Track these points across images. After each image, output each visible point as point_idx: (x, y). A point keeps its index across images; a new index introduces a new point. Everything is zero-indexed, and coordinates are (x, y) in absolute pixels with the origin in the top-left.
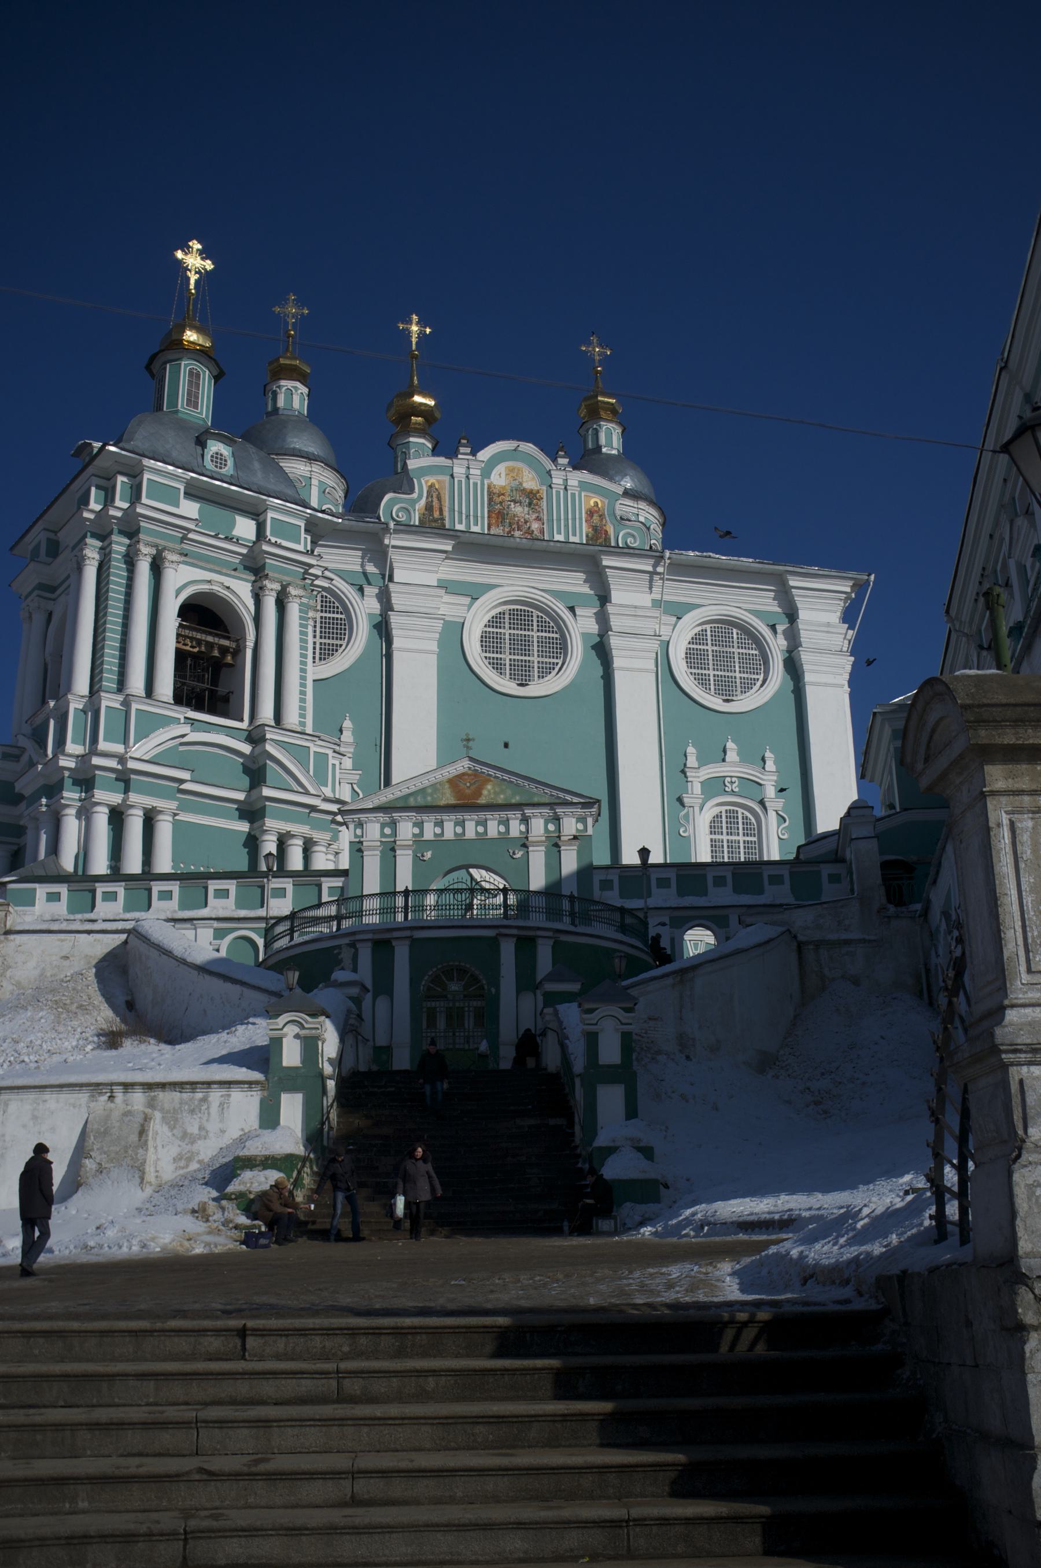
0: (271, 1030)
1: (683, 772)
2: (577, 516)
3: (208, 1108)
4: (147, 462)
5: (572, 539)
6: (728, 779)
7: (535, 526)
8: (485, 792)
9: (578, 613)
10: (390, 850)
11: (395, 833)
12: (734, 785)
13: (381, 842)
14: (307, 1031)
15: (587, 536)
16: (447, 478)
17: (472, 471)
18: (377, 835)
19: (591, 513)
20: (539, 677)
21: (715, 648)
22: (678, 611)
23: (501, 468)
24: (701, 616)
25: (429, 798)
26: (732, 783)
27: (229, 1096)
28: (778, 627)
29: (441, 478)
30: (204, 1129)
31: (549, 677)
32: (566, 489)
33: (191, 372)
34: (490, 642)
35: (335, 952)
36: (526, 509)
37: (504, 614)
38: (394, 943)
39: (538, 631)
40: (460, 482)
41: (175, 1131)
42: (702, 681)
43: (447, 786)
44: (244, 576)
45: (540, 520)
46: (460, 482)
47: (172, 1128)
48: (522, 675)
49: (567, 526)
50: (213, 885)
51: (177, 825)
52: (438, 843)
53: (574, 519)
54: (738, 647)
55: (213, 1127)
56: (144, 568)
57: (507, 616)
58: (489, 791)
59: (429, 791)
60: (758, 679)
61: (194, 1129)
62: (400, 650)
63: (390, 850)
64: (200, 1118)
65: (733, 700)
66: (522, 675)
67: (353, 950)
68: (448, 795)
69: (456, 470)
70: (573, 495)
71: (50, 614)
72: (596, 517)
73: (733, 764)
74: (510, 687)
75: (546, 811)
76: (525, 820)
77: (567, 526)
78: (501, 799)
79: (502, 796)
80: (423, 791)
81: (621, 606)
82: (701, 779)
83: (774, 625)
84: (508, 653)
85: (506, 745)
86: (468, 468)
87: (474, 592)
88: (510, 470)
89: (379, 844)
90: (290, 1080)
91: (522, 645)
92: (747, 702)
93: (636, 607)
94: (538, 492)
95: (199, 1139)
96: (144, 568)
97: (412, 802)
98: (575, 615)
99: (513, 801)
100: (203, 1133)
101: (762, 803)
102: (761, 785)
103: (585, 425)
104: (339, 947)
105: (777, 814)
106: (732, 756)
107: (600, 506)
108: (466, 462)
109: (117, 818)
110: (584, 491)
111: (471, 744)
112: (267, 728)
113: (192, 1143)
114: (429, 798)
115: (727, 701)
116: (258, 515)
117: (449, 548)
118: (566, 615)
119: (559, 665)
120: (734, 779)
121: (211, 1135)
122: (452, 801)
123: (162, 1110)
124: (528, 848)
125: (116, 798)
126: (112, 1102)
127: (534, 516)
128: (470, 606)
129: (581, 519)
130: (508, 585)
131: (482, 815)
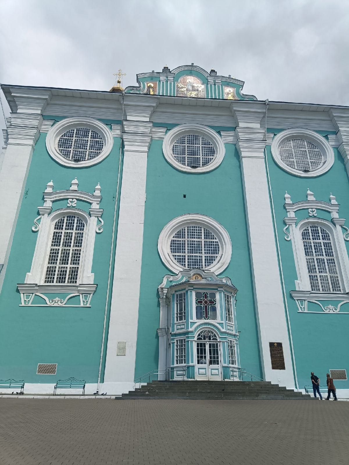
1: (285, 208)
6: (311, 210)
12: (314, 213)
22: (275, 131)
26: (313, 211)
32: (215, 85)
42: (291, 165)
48: (194, 164)
62: (127, 151)
66: (194, 164)
73: (312, 201)
82: (295, 210)
85: (185, 196)
87: (168, 127)
98: (221, 135)
101: (333, 222)
102: (329, 212)
105: (342, 227)
106: (310, 198)
117: (154, 105)
120: (313, 210)
128: (166, 132)
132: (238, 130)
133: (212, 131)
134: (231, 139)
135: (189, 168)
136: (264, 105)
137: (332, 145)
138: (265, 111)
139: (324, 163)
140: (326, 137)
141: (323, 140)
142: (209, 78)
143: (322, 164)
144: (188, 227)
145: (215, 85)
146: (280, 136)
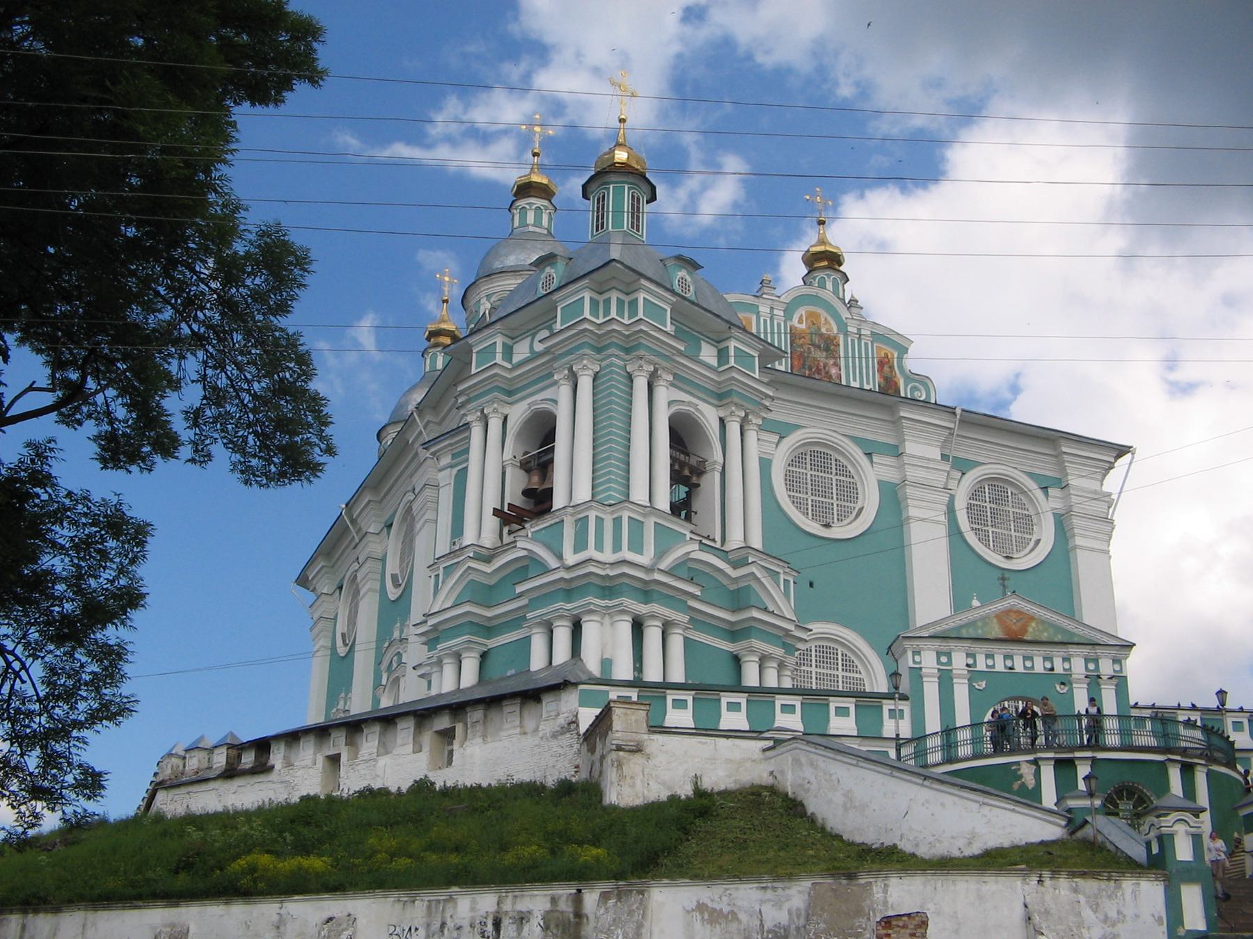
0: (1200, 827)
2: (871, 366)
3: (1123, 894)
4: (643, 282)
5: (853, 384)
7: (833, 371)
8: (1030, 629)
9: (874, 460)
10: (946, 680)
11: (950, 662)
13: (939, 670)
14: (1192, 829)
15: (879, 386)
16: (754, 318)
17: (776, 312)
18: (933, 662)
19: (881, 364)
20: (838, 519)
21: (992, 506)
22: (962, 466)
23: (802, 311)
24: (978, 475)
25: (980, 631)
27: (1139, 884)
28: (1049, 490)
29: (747, 315)
30: (1122, 913)
31: (848, 520)
32: (859, 339)
33: (633, 196)
34: (792, 482)
35: (1013, 768)
36: (824, 354)
37: (805, 454)
38: (1077, 763)
39: (837, 474)
40: (765, 321)
41: (1097, 914)
43: (995, 621)
44: (711, 401)
45: (837, 366)
46: (765, 321)
47: (1095, 911)
49: (861, 373)
50: (834, 703)
51: (687, 641)
52: (989, 675)
53: (867, 367)
54: (1013, 507)
55: (1129, 912)
56: (641, 384)
57: (808, 457)
58: (1034, 628)
59: (980, 624)
60: (1031, 539)
61: (1113, 914)
63: (946, 680)
64: (1117, 903)
65: (1012, 558)
67: (1034, 767)
68: (997, 629)
69: (761, 309)
70: (866, 344)
71: (506, 418)
72: (886, 368)
74: (814, 528)
75: (1085, 650)
76: (1066, 659)
77: (861, 373)
78: (1045, 636)
79: (1045, 634)
80: (972, 624)
81: (914, 457)
83: (1046, 488)
84: (810, 494)
85: (811, 585)
86: (772, 308)
88: (811, 315)
89: (936, 671)
90: (1189, 873)
91: (821, 489)
92: (1024, 562)
93: (929, 459)
94: (835, 338)
95: (1119, 922)
96: (641, 384)
97: (964, 633)
98: (872, 462)
99: (1056, 640)
100: (1121, 917)
103: (813, 273)
104: (1017, 763)
107: (890, 356)
108: (769, 302)
109: (638, 627)
110: (877, 342)
111: (1006, 583)
112: (750, 551)
113: (1113, 925)
114: (980, 631)
115: (1007, 557)
116: (718, 342)
118: (864, 461)
119: (857, 509)
121: (1128, 919)
122: (1002, 636)
123: (1084, 894)
124: (1072, 684)
125: (642, 609)
126: (1042, 885)
127: (832, 362)
128: (777, 444)
129: (873, 367)
130: (812, 427)
131: (1029, 650)
132: (906, 460)
133: (855, 448)
134: (891, 475)
135: (817, 525)
136: (951, 415)
137: (1053, 509)
138: (952, 425)
139: (1038, 542)
140: (1045, 489)
141: (1039, 494)
142: (849, 322)
143: (1032, 544)
144: (816, 646)
145: (859, 339)
146: (973, 475)
